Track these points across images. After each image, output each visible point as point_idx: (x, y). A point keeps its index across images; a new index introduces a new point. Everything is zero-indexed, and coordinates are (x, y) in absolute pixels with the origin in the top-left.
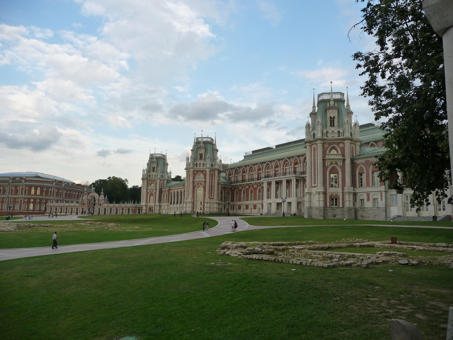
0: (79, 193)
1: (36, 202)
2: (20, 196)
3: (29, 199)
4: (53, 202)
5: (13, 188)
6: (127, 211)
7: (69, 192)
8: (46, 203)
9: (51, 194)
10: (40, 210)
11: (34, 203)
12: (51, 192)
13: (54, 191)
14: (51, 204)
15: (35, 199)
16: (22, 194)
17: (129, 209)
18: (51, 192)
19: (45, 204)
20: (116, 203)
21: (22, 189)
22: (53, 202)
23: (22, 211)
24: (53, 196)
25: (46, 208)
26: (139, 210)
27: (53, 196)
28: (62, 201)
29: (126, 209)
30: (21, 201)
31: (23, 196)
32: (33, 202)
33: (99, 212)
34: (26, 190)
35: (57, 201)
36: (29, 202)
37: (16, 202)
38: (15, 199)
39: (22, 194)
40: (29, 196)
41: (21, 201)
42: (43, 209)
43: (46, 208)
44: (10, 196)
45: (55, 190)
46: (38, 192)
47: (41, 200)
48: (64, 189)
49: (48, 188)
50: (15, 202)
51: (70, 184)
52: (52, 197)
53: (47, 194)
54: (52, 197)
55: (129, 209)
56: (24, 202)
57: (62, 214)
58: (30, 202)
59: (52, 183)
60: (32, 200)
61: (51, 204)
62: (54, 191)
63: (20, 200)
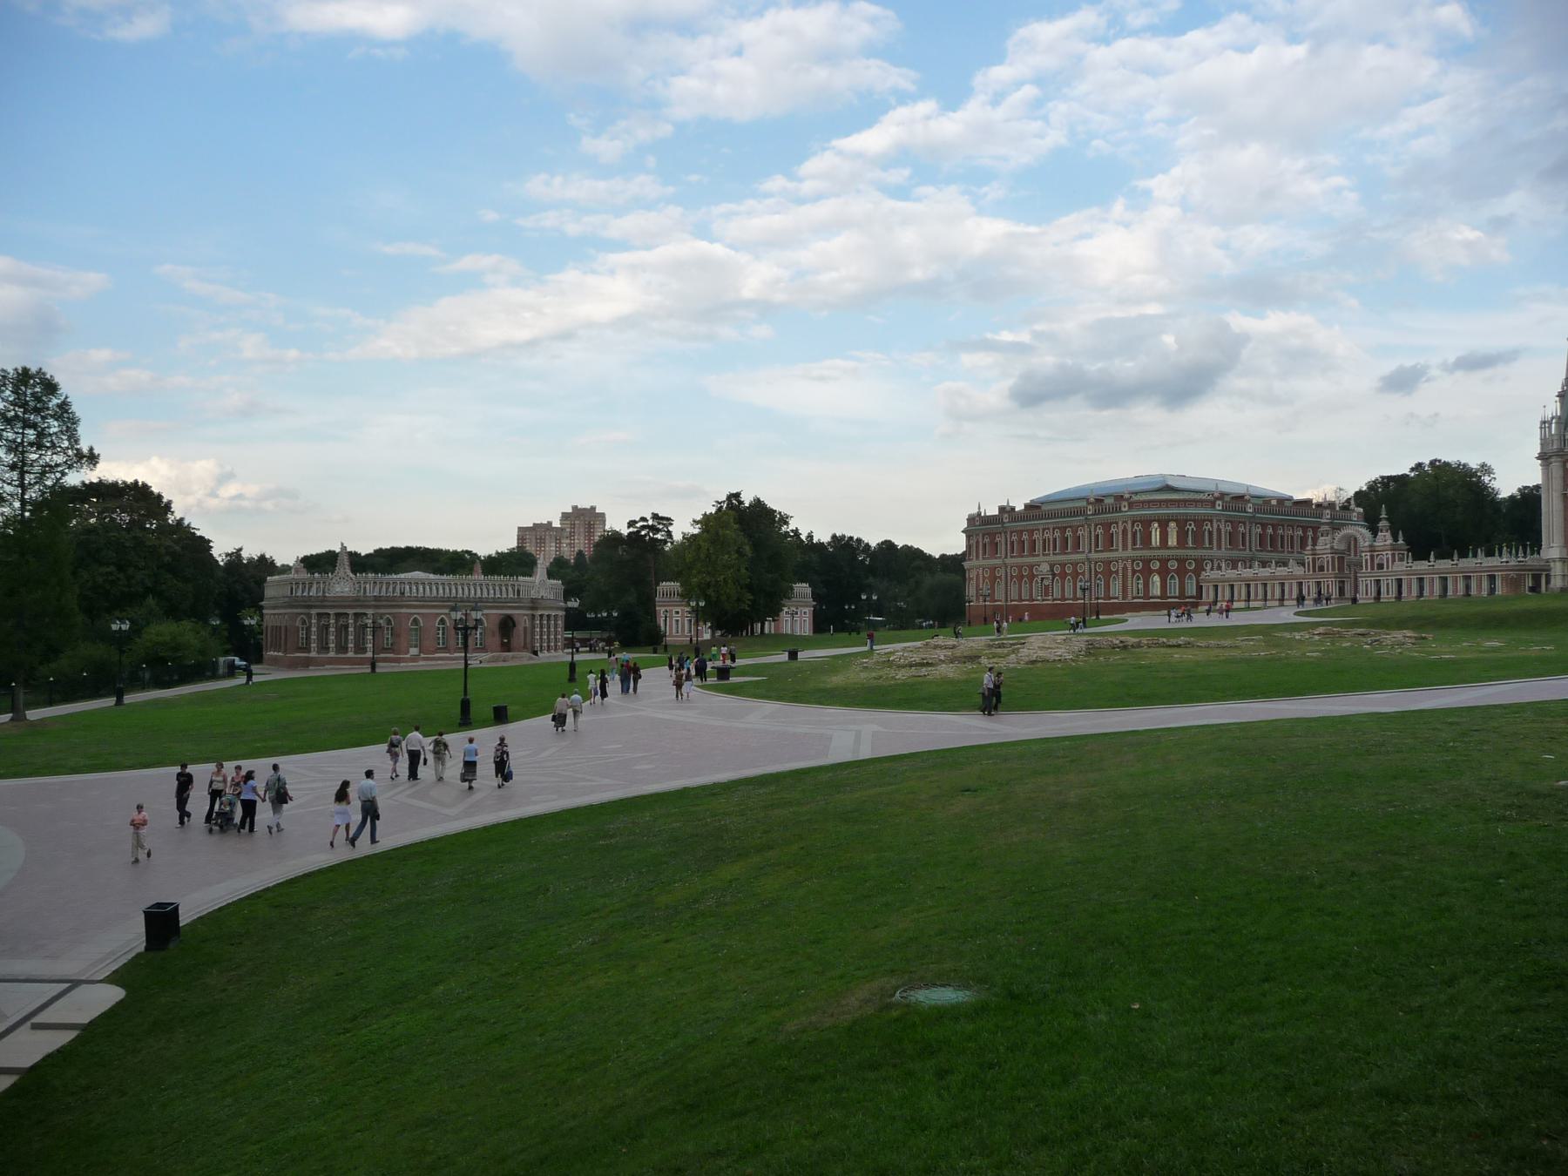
0: (1305, 532)
1: (1168, 571)
2: (1120, 554)
3: (1147, 562)
4: (1219, 568)
5: (1100, 531)
6: (1485, 584)
7: (1270, 531)
8: (1199, 569)
9: (1211, 542)
10: (1182, 595)
11: (1164, 573)
12: (1210, 533)
13: (1219, 530)
14: (1215, 574)
15: (1164, 562)
16: (1125, 547)
17: (1492, 578)
18: (1210, 533)
19: (1197, 576)
20: (1439, 557)
21: (1125, 532)
22: (1219, 568)
23: (1129, 600)
24: (1219, 547)
25: (1200, 589)
26: (1537, 578)
27: (1219, 547)
28: (1248, 563)
29: (1480, 579)
30: (1125, 569)
31: (1130, 553)
32: (1159, 572)
33: (1379, 592)
34: (1134, 534)
35: (1233, 564)
36: (1147, 572)
37: (1111, 573)
38: (1108, 563)
39: (1125, 547)
41: (1125, 569)
42: (1191, 589)
43: (1200, 589)
44: (1094, 555)
46: (1172, 541)
47: (1182, 561)
48: (1253, 520)
49: (1200, 522)
50: (1108, 574)
51: (1274, 502)
52: (1215, 552)
53: (1198, 543)
54: (1215, 552)
55: (1492, 578)
56: (1134, 572)
57: (1252, 604)
58: (1150, 572)
59: (1213, 504)
60: (1156, 565)
61: (1215, 574)
62: (1219, 530)
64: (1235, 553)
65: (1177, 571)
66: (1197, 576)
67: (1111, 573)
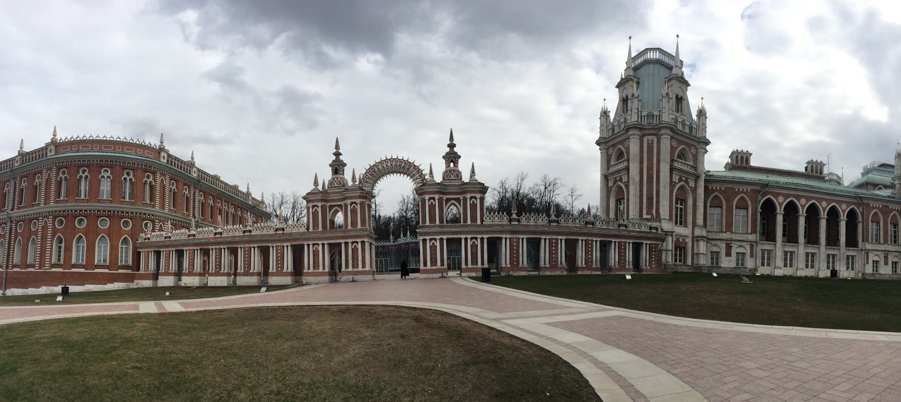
2: (42, 208)
8: (134, 234)
12: (152, 187)
15: (93, 217)
18: (152, 187)
19: (135, 240)
22: (161, 230)
24: (163, 206)
25: (137, 256)
27: (163, 206)
30: (45, 228)
31: (53, 206)
34: (59, 184)
37: (31, 233)
38: (29, 221)
40: (71, 206)
42: (126, 256)
43: (137, 256)
45: (166, 183)
63: (41, 224)
64: (179, 216)
65: (110, 232)
66: (135, 240)
67: (31, 233)
